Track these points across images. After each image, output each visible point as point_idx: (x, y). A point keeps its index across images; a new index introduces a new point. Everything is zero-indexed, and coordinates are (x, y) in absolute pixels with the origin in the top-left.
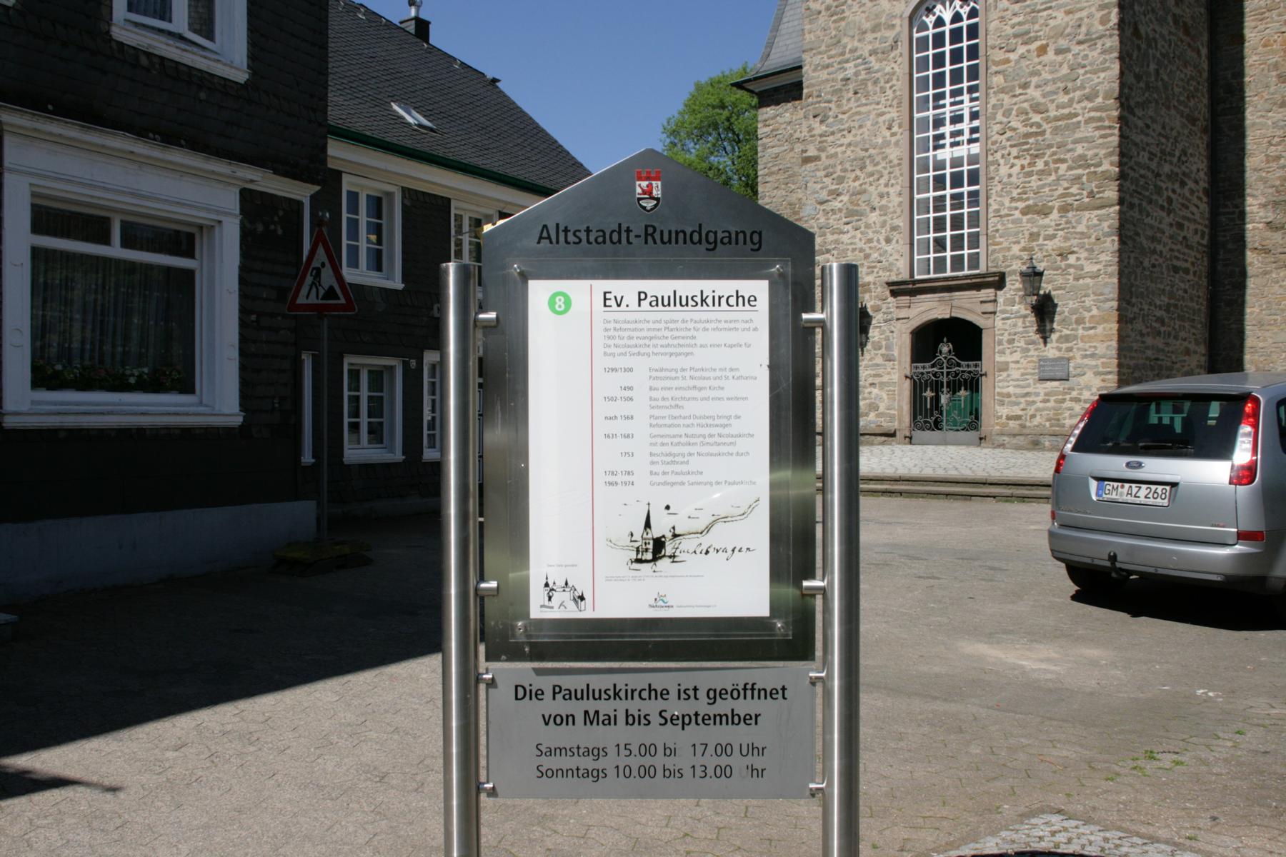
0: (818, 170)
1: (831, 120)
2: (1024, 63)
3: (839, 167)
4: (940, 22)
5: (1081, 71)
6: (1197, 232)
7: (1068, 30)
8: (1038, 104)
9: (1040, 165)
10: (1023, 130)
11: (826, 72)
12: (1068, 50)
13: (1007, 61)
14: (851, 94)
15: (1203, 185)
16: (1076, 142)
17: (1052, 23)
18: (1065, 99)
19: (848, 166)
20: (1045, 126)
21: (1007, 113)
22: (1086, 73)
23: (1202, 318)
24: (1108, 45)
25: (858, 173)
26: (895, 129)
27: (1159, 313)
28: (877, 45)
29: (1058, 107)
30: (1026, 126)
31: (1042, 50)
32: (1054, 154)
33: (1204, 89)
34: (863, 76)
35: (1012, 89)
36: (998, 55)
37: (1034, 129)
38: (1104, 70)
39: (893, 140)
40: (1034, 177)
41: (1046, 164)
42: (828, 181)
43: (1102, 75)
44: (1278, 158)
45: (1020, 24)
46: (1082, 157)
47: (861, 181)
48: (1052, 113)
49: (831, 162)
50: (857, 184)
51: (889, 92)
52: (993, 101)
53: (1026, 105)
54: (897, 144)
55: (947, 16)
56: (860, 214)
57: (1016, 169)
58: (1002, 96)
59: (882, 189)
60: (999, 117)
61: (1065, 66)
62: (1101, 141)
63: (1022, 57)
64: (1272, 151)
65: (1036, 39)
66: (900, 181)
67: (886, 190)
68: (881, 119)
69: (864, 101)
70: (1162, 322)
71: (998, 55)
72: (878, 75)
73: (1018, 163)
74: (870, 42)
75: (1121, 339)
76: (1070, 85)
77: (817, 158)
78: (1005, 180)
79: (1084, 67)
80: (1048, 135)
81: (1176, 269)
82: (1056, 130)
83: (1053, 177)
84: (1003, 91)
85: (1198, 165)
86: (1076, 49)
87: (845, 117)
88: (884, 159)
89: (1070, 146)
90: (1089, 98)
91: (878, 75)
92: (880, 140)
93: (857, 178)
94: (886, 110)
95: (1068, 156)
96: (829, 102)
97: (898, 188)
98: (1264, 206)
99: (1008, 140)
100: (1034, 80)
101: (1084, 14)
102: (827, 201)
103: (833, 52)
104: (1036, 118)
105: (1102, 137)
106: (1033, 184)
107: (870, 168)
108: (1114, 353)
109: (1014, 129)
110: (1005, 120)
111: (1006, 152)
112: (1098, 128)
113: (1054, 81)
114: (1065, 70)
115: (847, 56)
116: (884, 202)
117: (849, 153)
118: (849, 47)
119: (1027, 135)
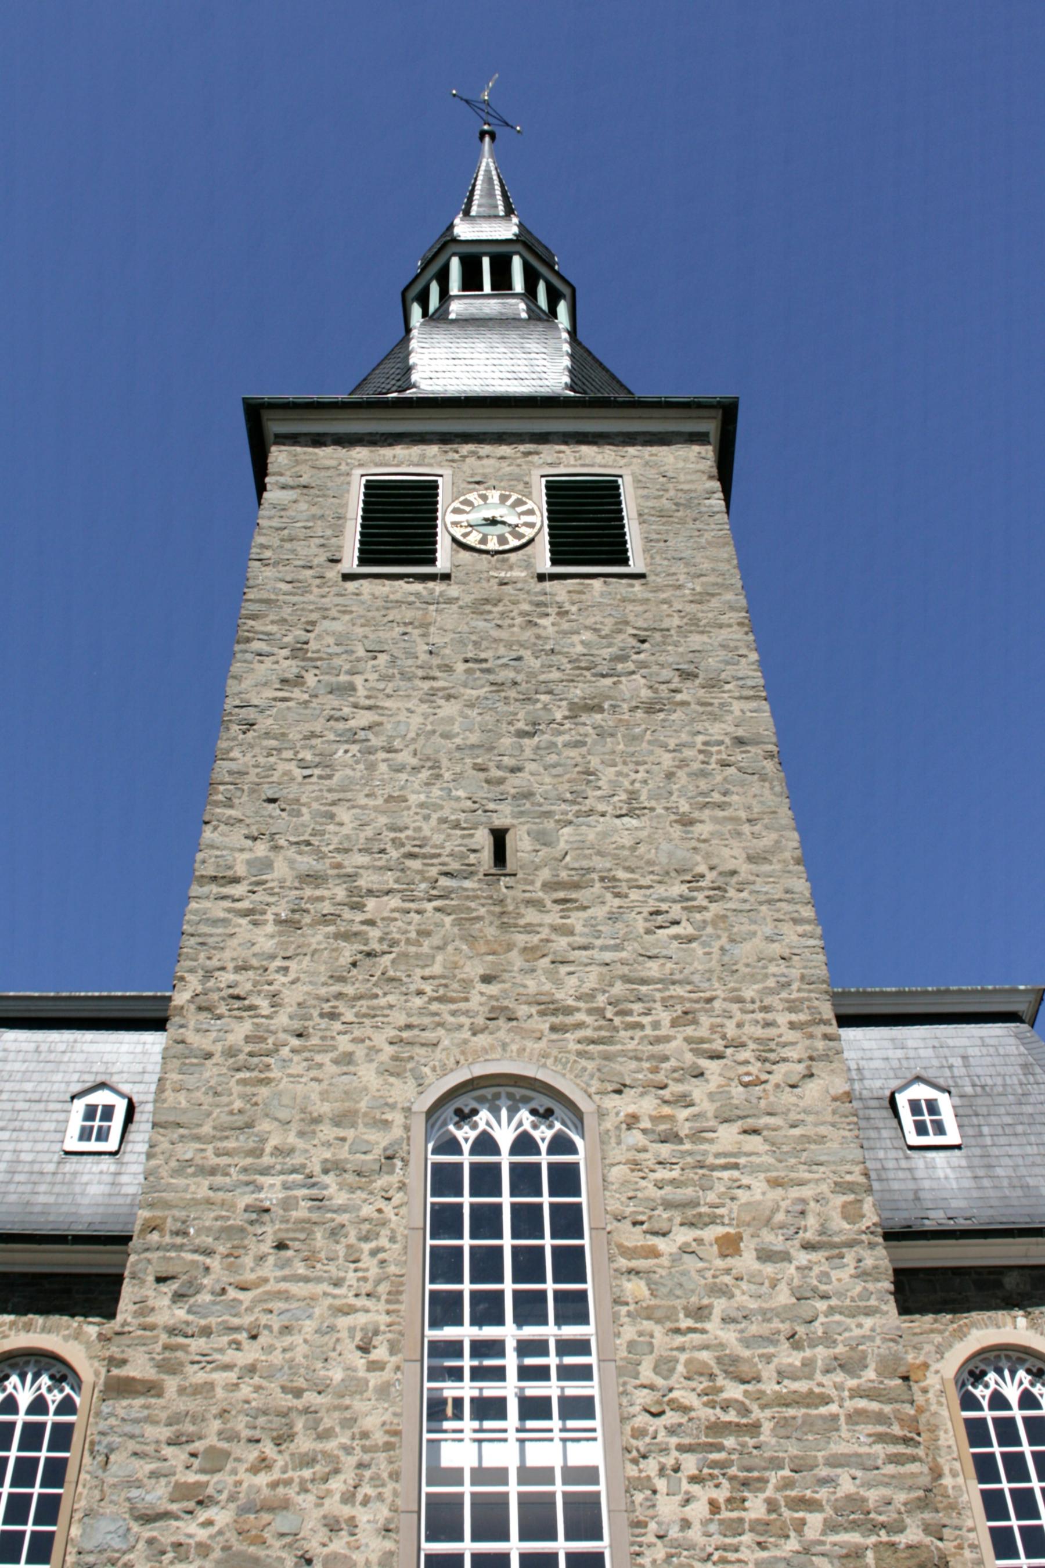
0: (150, 1420)
1: (205, 1297)
2: (691, 1263)
3: (216, 1425)
4: (486, 1144)
5: (821, 1305)
7: (780, 1217)
8: (735, 1360)
9: (756, 1508)
10: (707, 1414)
11: (206, 1183)
12: (785, 1257)
13: (653, 1253)
14: (266, 1247)
16: (836, 1462)
17: (743, 1196)
18: (795, 1359)
19: (240, 1424)
20: (757, 1413)
21: (664, 1366)
22: (831, 1310)
24: (869, 1262)
25: (269, 1449)
26: (380, 1353)
28: (344, 1153)
29: (782, 1375)
30: (712, 1405)
31: (730, 1246)
32: (788, 1484)
34: (302, 1212)
35: (670, 1315)
37: (731, 1416)
38: (869, 1312)
39: (375, 1379)
40: (747, 1538)
41: (772, 1506)
42: (177, 1456)
43: (868, 1322)
45: (673, 1182)
46: (854, 1502)
47: (276, 1475)
48: (770, 1387)
49: (192, 1405)
50: (262, 1479)
51: (368, 1262)
53: (705, 1356)
54: (384, 1391)
55: (505, 1136)
57: (698, 1510)
58: (648, 1325)
59: (334, 1506)
60: (646, 1373)
61: (783, 1289)
62: (890, 1469)
63: (685, 1250)
65: (714, 1220)
66: (387, 1491)
67: (346, 1511)
68: (343, 1322)
69: (301, 1269)
72: (343, 1218)
73: (703, 1494)
74: (328, 1144)
76: (801, 1330)
77: (153, 1389)
78: (674, 1533)
79: (825, 1297)
80: (766, 1435)
82: (783, 1424)
83: (793, 1544)
84: (648, 1314)
86: (803, 1258)
87: (246, 1297)
88: (349, 1423)
89: (823, 1472)
90: (848, 1365)
91: (343, 1218)
92: (337, 1375)
93: (263, 1464)
94: (359, 1302)
95: (823, 1494)
96: (208, 1252)
97: (383, 1512)
99: (671, 1431)
100: (720, 1306)
101: (807, 1192)
102: (166, 1515)
103: (231, 1144)
104: (734, 1391)
105: (895, 1459)
106: (744, 1554)
107: (304, 1443)
109: (685, 1409)
110: (660, 1382)
111: (669, 1461)
112: (881, 1438)
113: (766, 1315)
114: (783, 1297)
115: (266, 1160)
117: (245, 1391)
118: (273, 1142)
119: (717, 1428)
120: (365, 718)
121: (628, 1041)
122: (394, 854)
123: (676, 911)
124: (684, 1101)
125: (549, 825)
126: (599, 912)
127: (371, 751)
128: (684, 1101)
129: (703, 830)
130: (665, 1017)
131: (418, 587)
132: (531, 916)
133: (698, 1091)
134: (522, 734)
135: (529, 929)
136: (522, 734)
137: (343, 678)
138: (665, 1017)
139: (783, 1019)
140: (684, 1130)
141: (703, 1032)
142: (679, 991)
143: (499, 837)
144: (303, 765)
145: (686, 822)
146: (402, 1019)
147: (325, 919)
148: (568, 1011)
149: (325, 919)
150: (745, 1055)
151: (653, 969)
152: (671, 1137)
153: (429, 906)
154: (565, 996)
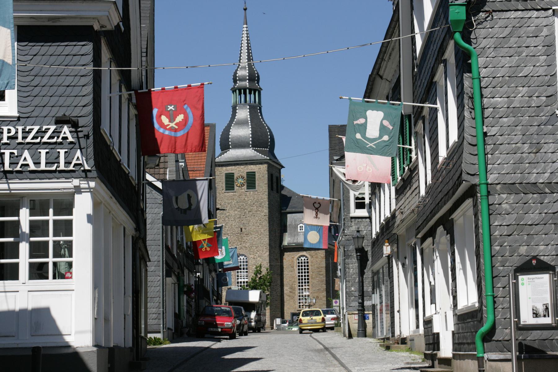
6: (279, 294)
15: (280, 285)
23: (280, 308)
27: (274, 308)
33: (279, 268)
36: (251, 267)
44: (291, 280)
52: (250, 274)
64: (290, 279)
70: (274, 309)
71: (251, 267)
75: (270, 312)
81: (276, 300)
85: (279, 282)
98: (289, 288)
108: (269, 315)
120: (228, 214)
121: (252, 250)
122: (232, 231)
123: (256, 237)
124: (256, 255)
126: (250, 237)
127: (229, 218)
128: (256, 255)
129: (260, 227)
130: (255, 248)
131: (232, 193)
132: (244, 238)
133: (257, 255)
134: (243, 215)
135: (244, 239)
136: (243, 215)
138: (255, 248)
139: (264, 248)
140: (255, 258)
142: (256, 245)
143: (241, 229)
144: (223, 221)
145: (258, 226)
151: (254, 243)
152: (254, 259)
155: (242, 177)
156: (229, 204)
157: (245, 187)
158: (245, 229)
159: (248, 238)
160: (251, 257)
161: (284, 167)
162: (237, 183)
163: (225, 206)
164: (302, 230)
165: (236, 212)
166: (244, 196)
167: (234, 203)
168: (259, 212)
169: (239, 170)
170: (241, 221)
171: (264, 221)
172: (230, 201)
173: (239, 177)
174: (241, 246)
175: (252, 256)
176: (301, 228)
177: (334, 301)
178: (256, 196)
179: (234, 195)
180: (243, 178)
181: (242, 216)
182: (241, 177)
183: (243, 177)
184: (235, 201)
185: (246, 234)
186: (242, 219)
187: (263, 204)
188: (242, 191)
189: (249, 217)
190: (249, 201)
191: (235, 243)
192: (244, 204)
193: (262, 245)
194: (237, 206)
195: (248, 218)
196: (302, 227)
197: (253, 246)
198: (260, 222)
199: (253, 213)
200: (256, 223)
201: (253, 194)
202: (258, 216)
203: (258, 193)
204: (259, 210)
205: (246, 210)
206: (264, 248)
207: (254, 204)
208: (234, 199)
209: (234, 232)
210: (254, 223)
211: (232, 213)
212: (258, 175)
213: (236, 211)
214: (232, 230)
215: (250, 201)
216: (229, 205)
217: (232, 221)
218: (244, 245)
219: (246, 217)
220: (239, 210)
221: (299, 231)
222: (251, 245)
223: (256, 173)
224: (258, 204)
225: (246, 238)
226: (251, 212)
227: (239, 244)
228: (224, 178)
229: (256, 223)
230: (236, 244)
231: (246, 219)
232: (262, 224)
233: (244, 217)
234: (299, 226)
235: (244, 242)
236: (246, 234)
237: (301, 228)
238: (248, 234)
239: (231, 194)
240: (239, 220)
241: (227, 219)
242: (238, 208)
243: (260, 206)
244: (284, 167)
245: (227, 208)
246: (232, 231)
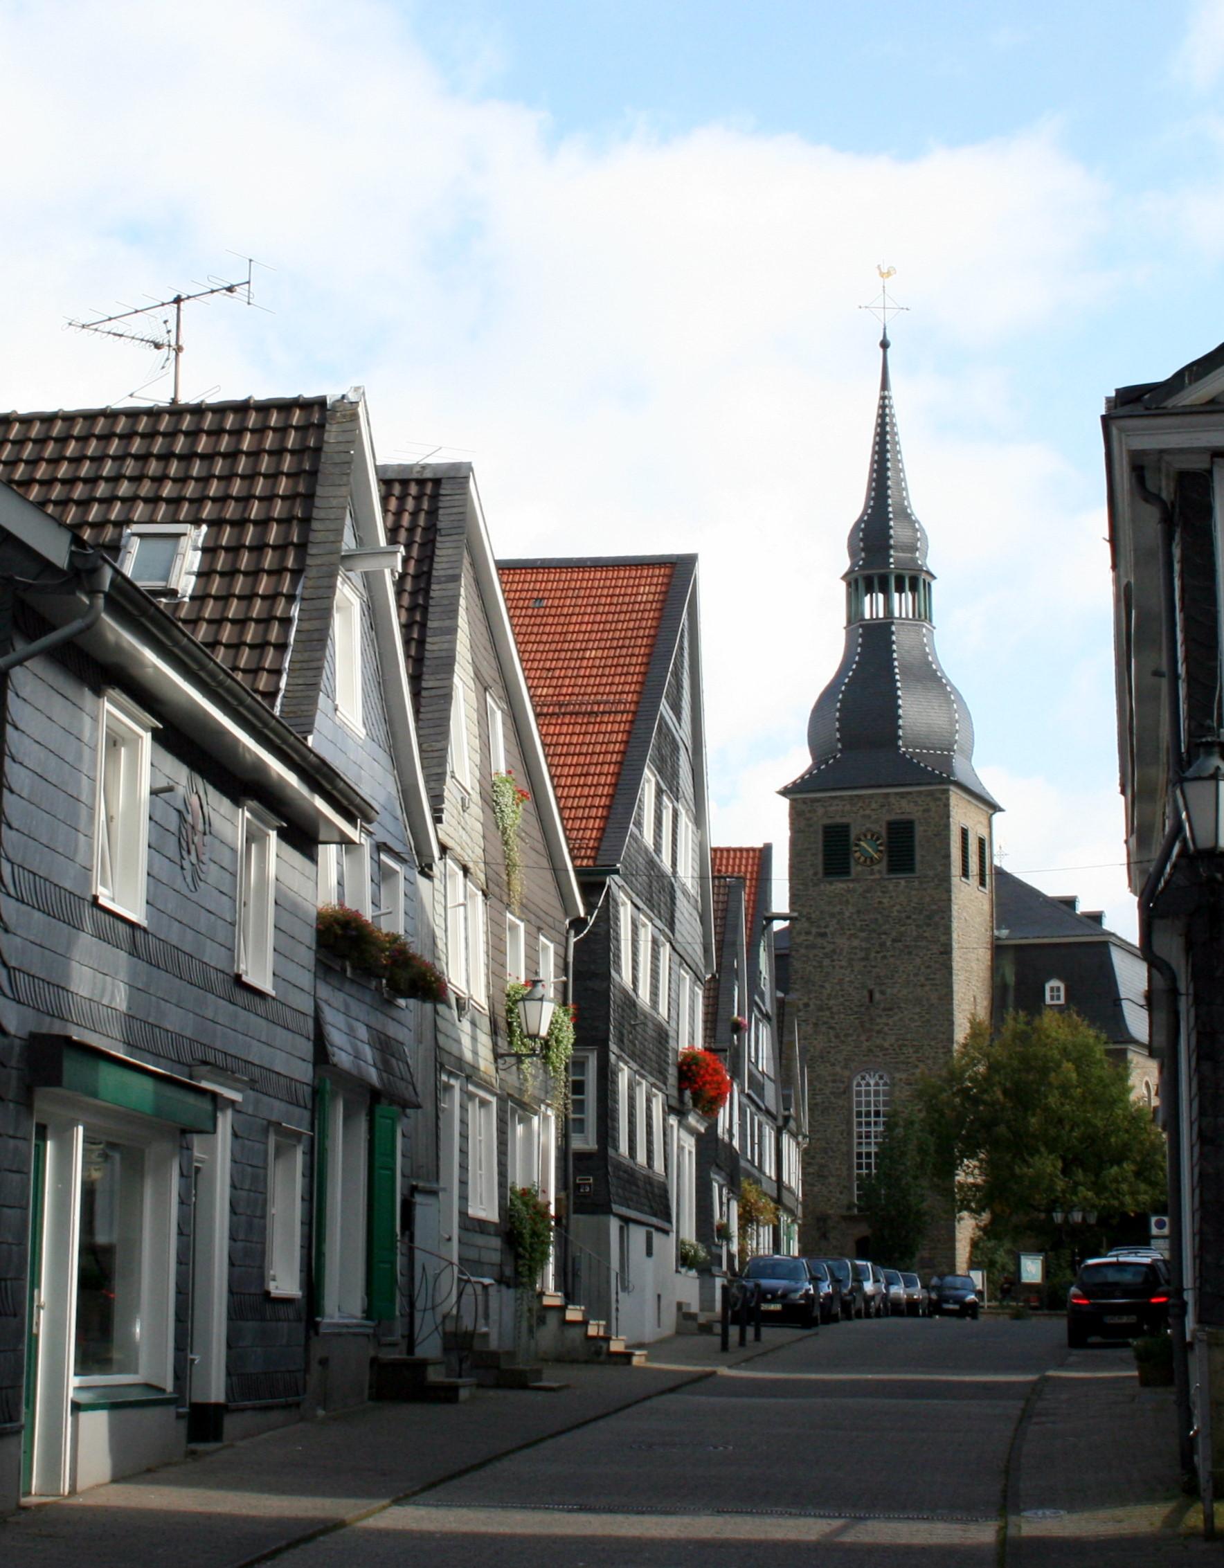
34: (827, 1104)
56: (825, 1177)
68: (837, 1129)
92: (836, 1140)
116: (839, 1173)
122: (842, 1000)
123: (916, 1017)
125: (883, 987)
126: (896, 1018)
127: (833, 961)
128: (913, 1074)
129: (927, 988)
130: (911, 1050)
132: (878, 1020)
134: (878, 952)
135: (878, 1024)
137: (823, 930)
138: (911, 1050)
139: (941, 1051)
141: (919, 1055)
143: (871, 993)
144: (814, 967)
145: (922, 986)
146: (845, 1053)
147: (825, 1023)
148: (887, 1049)
149: (825, 1023)
150: (929, 1062)
151: (909, 1036)
153: (852, 1017)
154: (886, 1045)
155: (872, 836)
156: (832, 915)
157: (883, 865)
158: (883, 993)
159: (890, 1022)
160: (901, 1080)
161: (1001, 810)
162: (857, 855)
163: (822, 923)
164: (1059, 998)
165: (856, 943)
166: (879, 894)
167: (847, 914)
168: (924, 943)
169: (864, 816)
170: (870, 968)
171: (940, 970)
172: (837, 909)
173: (865, 836)
174: (868, 1044)
175: (904, 1076)
176: (1055, 994)
177: (1154, 1219)
178: (914, 893)
179: (849, 891)
180: (878, 839)
181: (873, 955)
182: (869, 837)
183: (875, 837)
184: (851, 909)
185: (884, 1010)
186: (873, 964)
187: (937, 918)
188: (872, 877)
189: (892, 956)
190: (895, 908)
191: (850, 1035)
192: (879, 916)
193: (933, 1043)
194: (858, 924)
195: (892, 960)
196: (1058, 989)
197: (905, 1046)
198: (929, 971)
199: (907, 947)
200: (916, 975)
201: (907, 887)
202: (921, 954)
203: (921, 883)
204: (925, 934)
205: (883, 936)
206: (941, 1051)
207: (909, 917)
208: (847, 902)
209: (847, 1003)
210: (909, 975)
211: (842, 941)
212: (922, 828)
213: (856, 938)
214: (843, 996)
215: (898, 907)
216: (835, 921)
217: (841, 967)
218: (878, 1041)
219: (884, 957)
220: (863, 935)
221: (1048, 1001)
222: (901, 1042)
223: (916, 823)
224: (922, 917)
225: (884, 1020)
226: (900, 941)
227: (863, 1038)
228: (820, 837)
229: (916, 975)
230: (854, 1038)
231: (886, 962)
232: (933, 979)
233: (879, 956)
234: (1048, 986)
235: (879, 1032)
236: (884, 1010)
237: (1055, 994)
238: (890, 1009)
239: (839, 886)
240: (865, 967)
241: (826, 962)
242: (862, 930)
243: (929, 925)
244: (1001, 810)
245: (827, 930)
246: (842, 1000)
